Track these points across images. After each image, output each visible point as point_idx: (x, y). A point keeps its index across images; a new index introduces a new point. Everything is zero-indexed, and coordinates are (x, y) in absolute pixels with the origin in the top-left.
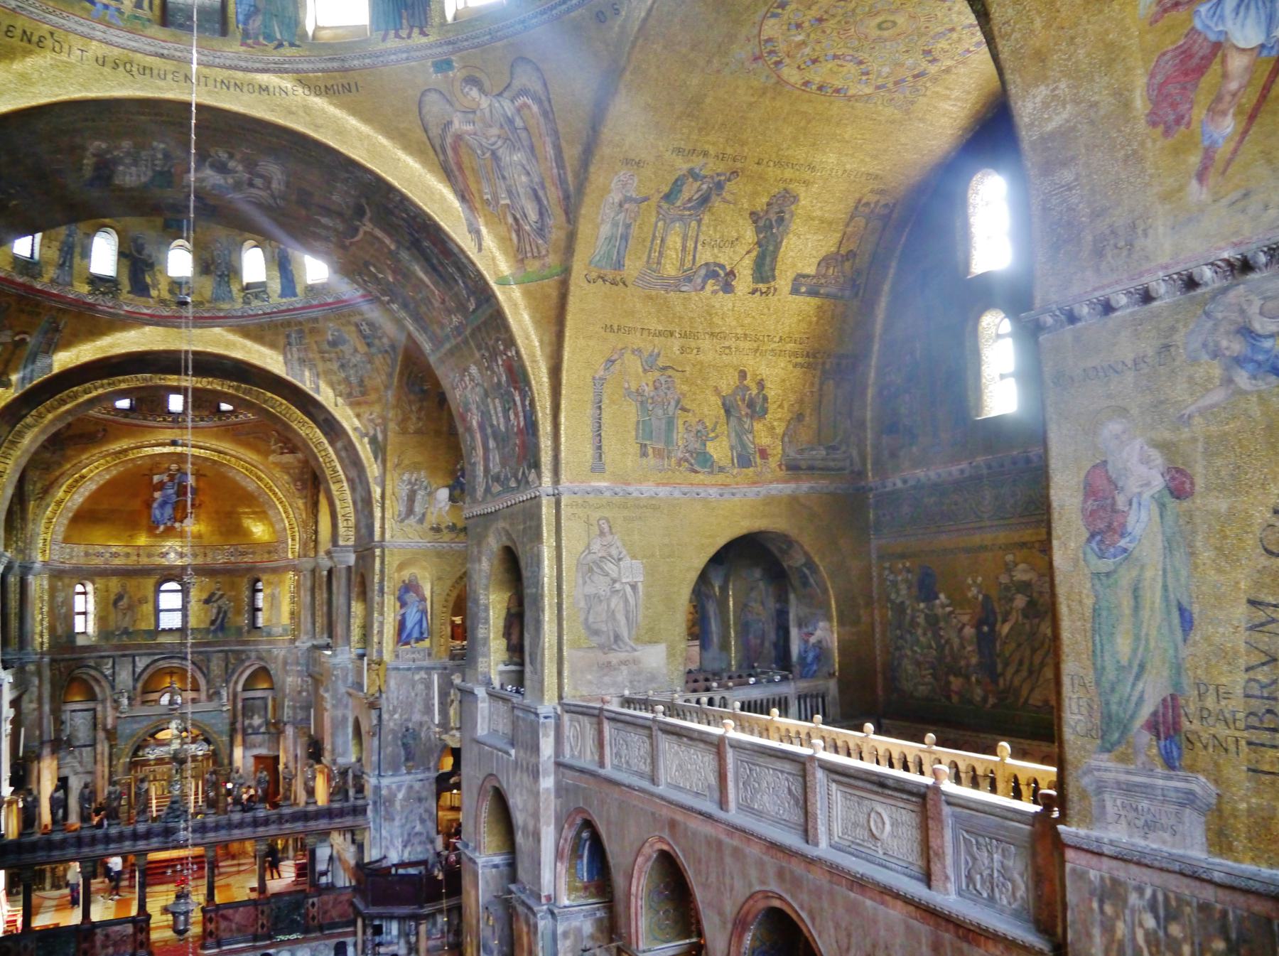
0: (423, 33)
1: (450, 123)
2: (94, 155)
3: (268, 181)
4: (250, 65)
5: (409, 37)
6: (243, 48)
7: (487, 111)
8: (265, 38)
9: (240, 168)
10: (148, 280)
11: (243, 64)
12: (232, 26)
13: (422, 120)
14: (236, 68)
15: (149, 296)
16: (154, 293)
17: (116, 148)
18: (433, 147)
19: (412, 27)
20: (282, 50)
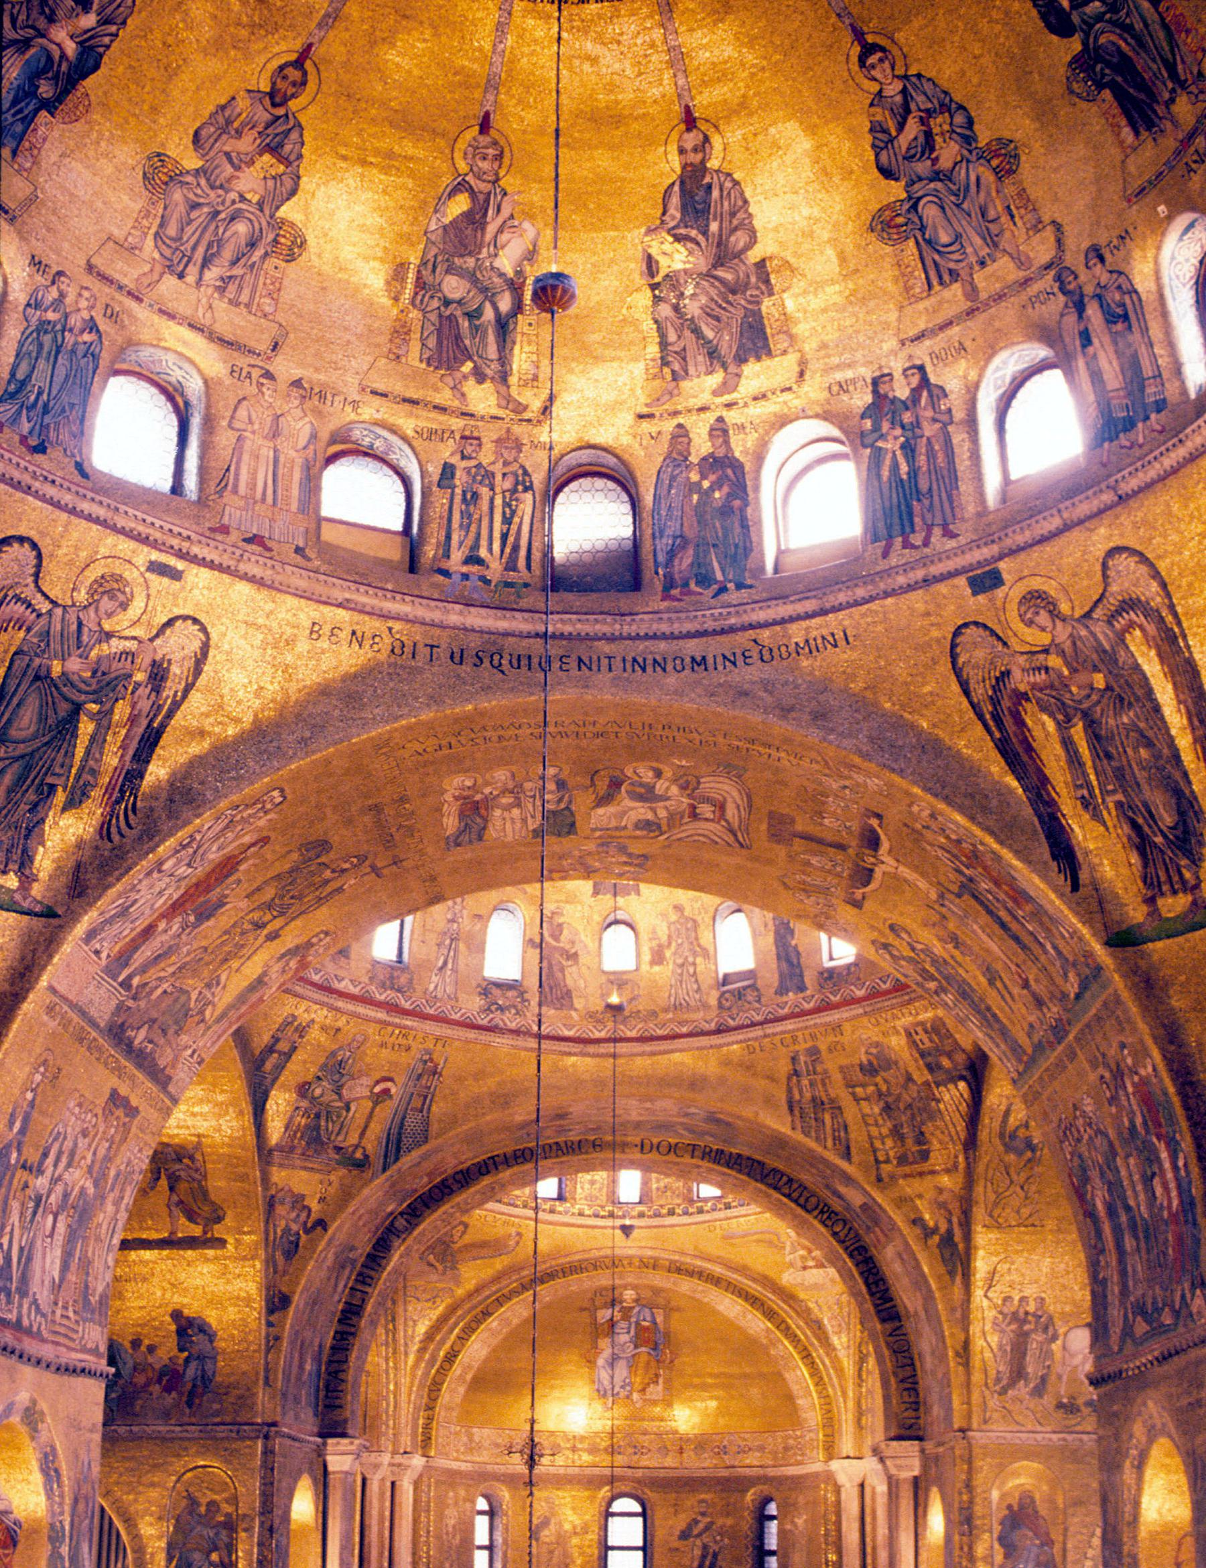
0: (949, 534)
1: (1006, 674)
2: (456, 798)
3: (721, 807)
4: (677, 628)
5: (926, 543)
6: (666, 604)
7: (1067, 646)
8: (698, 583)
9: (674, 790)
10: (570, 982)
11: (664, 628)
12: (647, 573)
13: (957, 671)
14: (655, 637)
15: (572, 1007)
16: (578, 1003)
17: (487, 784)
18: (980, 716)
19: (929, 529)
20: (724, 597)
